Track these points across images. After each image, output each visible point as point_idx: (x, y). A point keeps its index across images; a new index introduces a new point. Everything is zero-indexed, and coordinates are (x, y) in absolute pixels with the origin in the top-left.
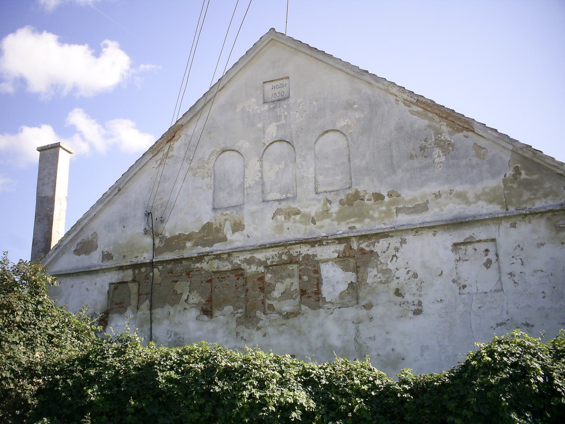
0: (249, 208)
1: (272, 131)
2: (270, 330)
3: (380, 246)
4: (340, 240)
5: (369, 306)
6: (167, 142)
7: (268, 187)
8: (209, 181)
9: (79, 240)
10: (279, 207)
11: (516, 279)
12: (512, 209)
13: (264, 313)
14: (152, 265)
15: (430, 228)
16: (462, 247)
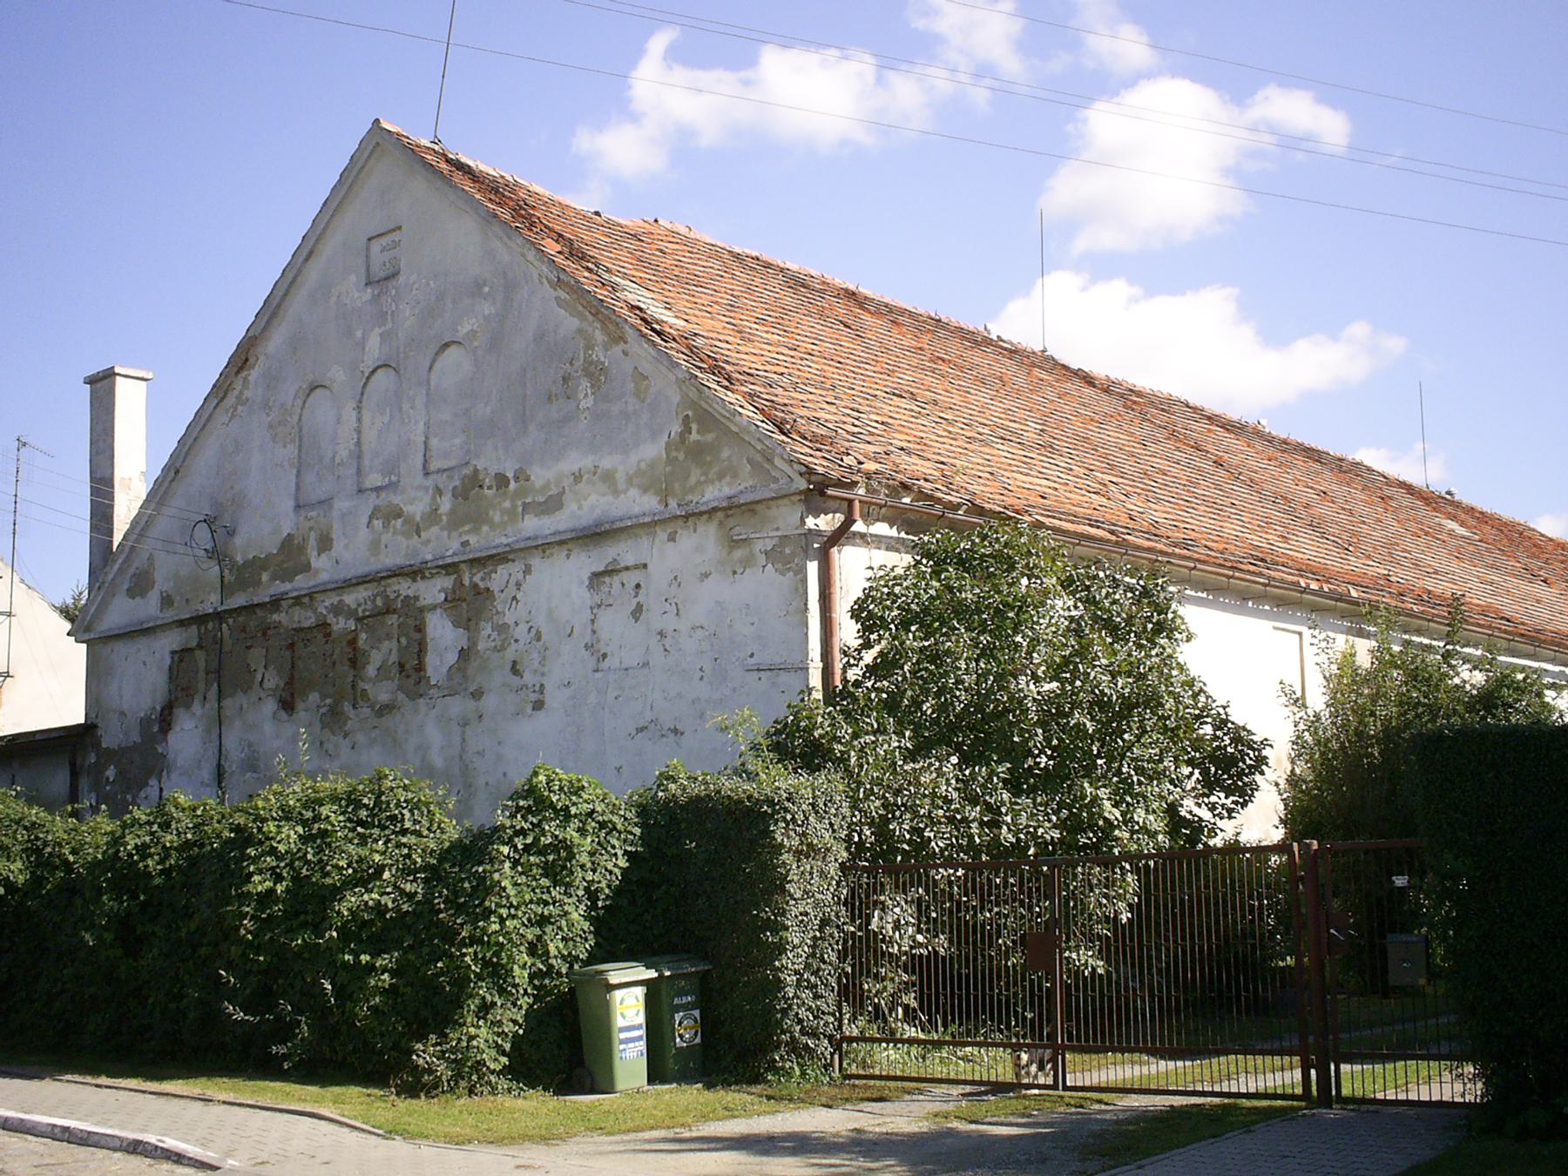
0: (342, 505)
1: (374, 348)
2: (360, 738)
3: (499, 578)
4: (450, 568)
5: (477, 695)
6: (238, 373)
7: (366, 462)
8: (292, 450)
9: (132, 571)
10: (377, 502)
11: (668, 642)
12: (673, 504)
13: (354, 707)
14: (219, 616)
15: (561, 543)
16: (607, 579)
